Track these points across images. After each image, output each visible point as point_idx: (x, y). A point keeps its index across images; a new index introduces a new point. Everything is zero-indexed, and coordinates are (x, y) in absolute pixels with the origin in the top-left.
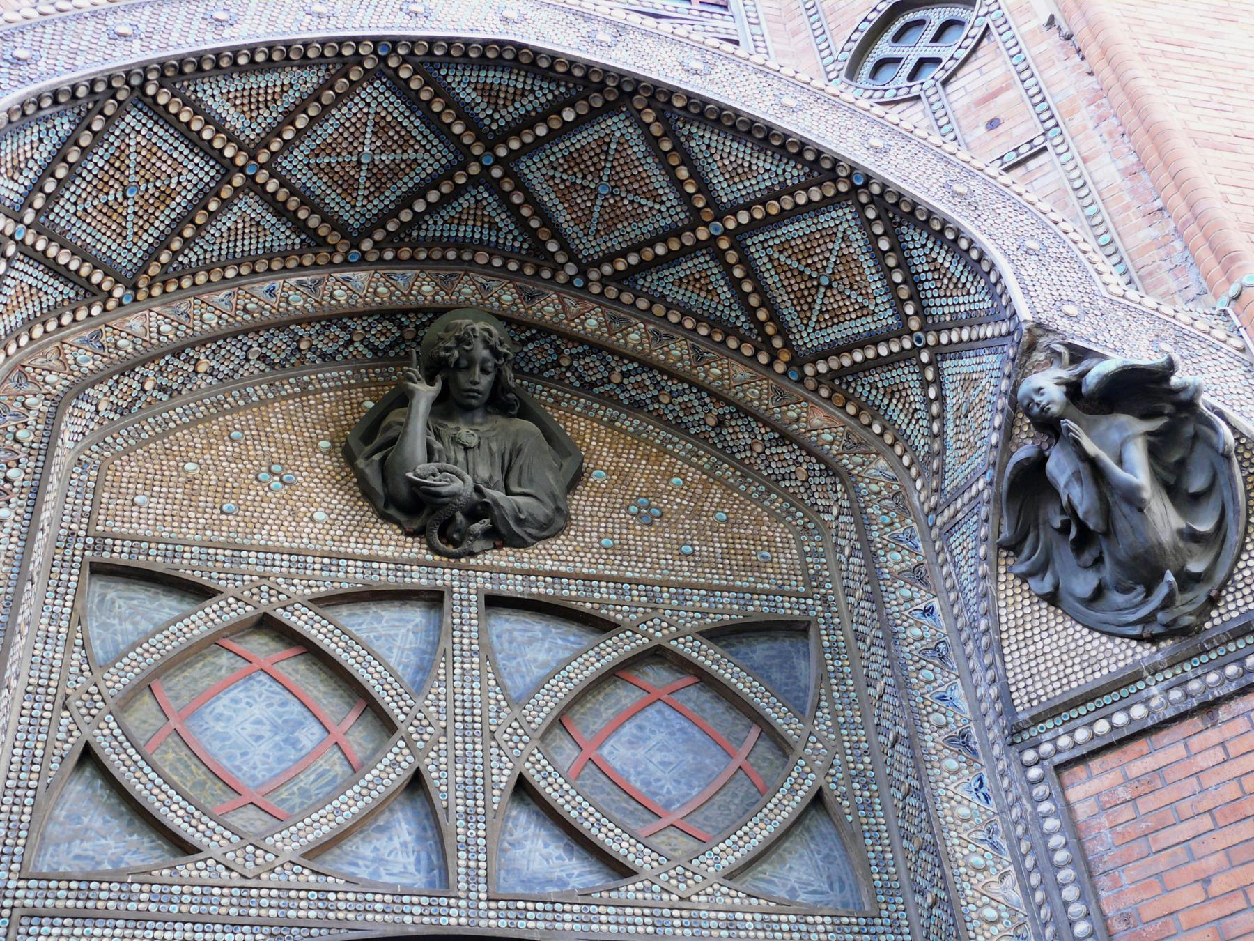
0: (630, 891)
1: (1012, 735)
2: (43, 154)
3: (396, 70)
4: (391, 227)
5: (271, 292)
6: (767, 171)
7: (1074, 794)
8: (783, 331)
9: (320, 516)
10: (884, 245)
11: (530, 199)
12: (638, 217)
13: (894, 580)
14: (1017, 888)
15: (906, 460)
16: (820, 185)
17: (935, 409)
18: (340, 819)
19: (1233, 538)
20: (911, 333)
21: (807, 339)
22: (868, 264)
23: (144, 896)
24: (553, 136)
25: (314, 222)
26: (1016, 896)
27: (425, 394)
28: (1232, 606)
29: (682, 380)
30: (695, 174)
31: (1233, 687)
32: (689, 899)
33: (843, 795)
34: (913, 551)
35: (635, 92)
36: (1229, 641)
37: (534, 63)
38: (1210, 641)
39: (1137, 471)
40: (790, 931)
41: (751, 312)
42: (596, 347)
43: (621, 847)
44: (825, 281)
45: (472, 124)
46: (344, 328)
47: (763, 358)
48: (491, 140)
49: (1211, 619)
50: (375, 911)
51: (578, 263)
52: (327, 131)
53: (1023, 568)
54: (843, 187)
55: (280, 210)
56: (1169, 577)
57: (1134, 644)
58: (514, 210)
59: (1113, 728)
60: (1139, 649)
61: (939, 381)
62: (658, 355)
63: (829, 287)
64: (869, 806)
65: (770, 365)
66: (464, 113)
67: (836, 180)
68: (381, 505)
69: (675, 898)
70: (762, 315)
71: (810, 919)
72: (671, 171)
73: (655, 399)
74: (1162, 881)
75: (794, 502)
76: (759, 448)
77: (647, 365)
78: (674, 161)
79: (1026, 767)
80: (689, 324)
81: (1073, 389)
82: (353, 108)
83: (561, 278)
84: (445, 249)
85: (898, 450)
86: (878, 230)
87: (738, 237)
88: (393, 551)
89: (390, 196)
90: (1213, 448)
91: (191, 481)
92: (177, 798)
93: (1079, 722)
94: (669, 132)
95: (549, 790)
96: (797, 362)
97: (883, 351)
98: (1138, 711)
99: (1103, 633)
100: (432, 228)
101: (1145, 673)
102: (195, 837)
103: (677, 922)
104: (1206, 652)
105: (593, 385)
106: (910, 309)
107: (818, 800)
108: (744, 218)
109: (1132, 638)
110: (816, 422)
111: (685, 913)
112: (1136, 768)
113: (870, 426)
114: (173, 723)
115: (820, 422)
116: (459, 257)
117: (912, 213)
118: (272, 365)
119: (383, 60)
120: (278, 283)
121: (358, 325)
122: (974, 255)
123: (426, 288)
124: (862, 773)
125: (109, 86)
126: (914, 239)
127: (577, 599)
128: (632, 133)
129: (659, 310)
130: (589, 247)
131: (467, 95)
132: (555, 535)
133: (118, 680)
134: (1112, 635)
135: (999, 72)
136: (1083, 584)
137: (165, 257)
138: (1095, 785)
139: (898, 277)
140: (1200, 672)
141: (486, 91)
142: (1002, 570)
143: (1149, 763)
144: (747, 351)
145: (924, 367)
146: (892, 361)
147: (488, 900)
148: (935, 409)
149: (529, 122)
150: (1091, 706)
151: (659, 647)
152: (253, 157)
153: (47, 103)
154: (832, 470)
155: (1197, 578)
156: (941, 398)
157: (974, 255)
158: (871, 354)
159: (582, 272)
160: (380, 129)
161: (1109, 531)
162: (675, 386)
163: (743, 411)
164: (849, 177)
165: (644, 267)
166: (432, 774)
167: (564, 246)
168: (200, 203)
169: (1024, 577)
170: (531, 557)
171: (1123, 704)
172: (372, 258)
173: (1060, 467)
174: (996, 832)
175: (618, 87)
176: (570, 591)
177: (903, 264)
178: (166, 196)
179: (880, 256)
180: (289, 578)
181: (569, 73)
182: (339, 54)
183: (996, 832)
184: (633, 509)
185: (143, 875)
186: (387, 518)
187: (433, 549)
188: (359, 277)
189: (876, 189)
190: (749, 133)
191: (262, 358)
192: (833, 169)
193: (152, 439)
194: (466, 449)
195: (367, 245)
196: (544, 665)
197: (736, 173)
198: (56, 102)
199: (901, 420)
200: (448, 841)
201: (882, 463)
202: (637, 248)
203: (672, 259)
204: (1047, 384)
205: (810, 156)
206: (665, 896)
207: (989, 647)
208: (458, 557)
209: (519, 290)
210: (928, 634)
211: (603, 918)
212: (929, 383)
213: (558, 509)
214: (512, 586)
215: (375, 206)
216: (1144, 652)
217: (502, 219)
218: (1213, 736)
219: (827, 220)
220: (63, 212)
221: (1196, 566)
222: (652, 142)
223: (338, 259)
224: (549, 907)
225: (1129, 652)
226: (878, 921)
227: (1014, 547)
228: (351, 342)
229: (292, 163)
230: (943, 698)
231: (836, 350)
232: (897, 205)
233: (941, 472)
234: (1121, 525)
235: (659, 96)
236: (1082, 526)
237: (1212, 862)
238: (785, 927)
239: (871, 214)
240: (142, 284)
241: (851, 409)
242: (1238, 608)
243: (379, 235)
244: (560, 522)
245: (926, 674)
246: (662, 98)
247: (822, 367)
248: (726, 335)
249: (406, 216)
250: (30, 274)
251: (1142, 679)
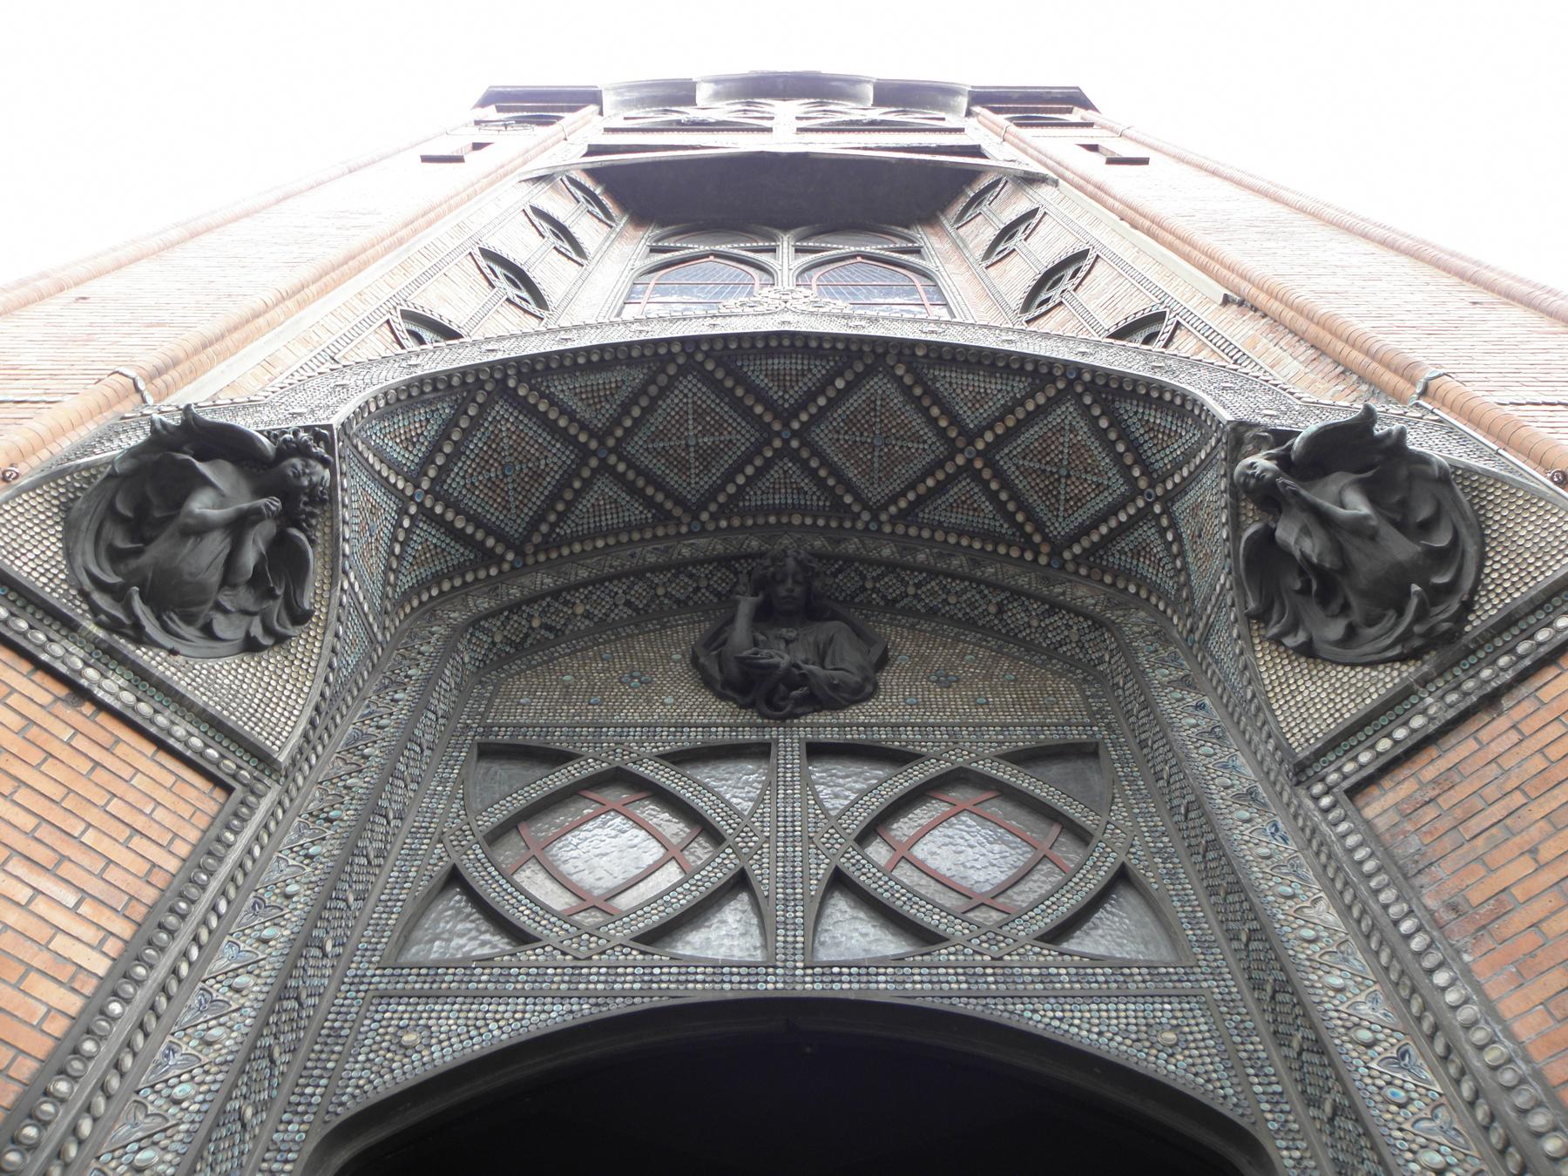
0: (943, 954)
1: (1296, 774)
2: (432, 430)
3: (702, 364)
4: (722, 499)
5: (633, 556)
6: (998, 391)
8: (1040, 527)
9: (669, 700)
10: (1104, 423)
11: (825, 462)
12: (908, 460)
13: (1164, 687)
14: (1332, 910)
15: (1161, 606)
16: (1042, 390)
17: (1175, 549)
18: (669, 910)
19: (1471, 550)
20: (1142, 492)
21: (1060, 527)
22: (1094, 445)
23: (484, 978)
24: (833, 403)
25: (660, 497)
26: (1332, 918)
27: (746, 606)
28: (1488, 607)
29: (963, 579)
30: (946, 411)
31: (1508, 676)
32: (1001, 959)
33: (1146, 868)
34: (1179, 667)
35: (886, 353)
36: (1493, 637)
37: (806, 346)
38: (1475, 640)
39: (1358, 506)
40: (1106, 982)
41: (1010, 517)
42: (891, 566)
43: (933, 920)
44: (1063, 472)
45: (770, 405)
46: (691, 576)
47: (1029, 556)
48: (787, 416)
49: (1470, 622)
50: (696, 982)
51: (870, 509)
52: (657, 420)
53: (1274, 631)
54: (1061, 385)
55: (632, 489)
56: (1415, 588)
57: (1397, 665)
58: (813, 473)
59: (1396, 742)
60: (1404, 668)
61: (1173, 525)
62: (942, 565)
63: (1068, 476)
64: (1172, 875)
65: (1035, 560)
66: (761, 396)
67: (1054, 380)
68: (718, 687)
69: (987, 958)
70: (1020, 518)
71: (1126, 971)
72: (925, 411)
73: (945, 601)
74: (1484, 863)
75: (1072, 663)
76: (1035, 623)
77: (933, 573)
78: (926, 402)
79: (1316, 799)
80: (964, 542)
81: (1284, 461)
82: (675, 398)
83: (860, 525)
84: (767, 516)
85: (1153, 600)
86: (1096, 412)
87: (987, 455)
89: (716, 473)
90: (1428, 478)
91: (567, 687)
92: (525, 901)
93: (1360, 748)
94: (919, 380)
95: (863, 878)
96: (1056, 552)
97: (1123, 517)
98: (1417, 722)
99: (1365, 665)
100: (754, 499)
101: (1416, 687)
103: (991, 979)
104: (1474, 652)
105: (895, 601)
106: (1136, 472)
107: (1122, 877)
108: (989, 437)
109: (1393, 660)
110: (1080, 593)
111: (999, 971)
112: (1430, 773)
113: (1126, 589)
114: (532, 852)
115: (1085, 595)
116: (779, 521)
117: (1121, 387)
118: (636, 610)
119: (690, 356)
120: (638, 550)
121: (702, 571)
122: (1178, 401)
123: (754, 543)
124: (1160, 851)
125: (478, 379)
126: (1127, 409)
127: (886, 740)
128: (891, 388)
129: (939, 536)
130: (876, 494)
131: (762, 381)
132: (867, 699)
133: (487, 821)
134: (1373, 665)
136: (1336, 630)
137: (544, 528)
138: (1391, 798)
139: (1121, 448)
140: (1472, 672)
141: (775, 376)
142: (1257, 641)
143: (1443, 764)
144: (1015, 553)
145: (1158, 517)
146: (1133, 522)
147: (804, 968)
148: (1175, 549)
149: (811, 397)
150: (1369, 730)
151: (961, 769)
152: (602, 443)
153: (428, 389)
154: (1098, 624)
155: (1450, 589)
156: (1178, 538)
157: (1178, 401)
158: (1113, 523)
159: (875, 518)
160: (699, 416)
161: (1346, 568)
162: (957, 586)
163: (1017, 593)
164: (1064, 375)
165: (921, 501)
166: (755, 870)
167: (858, 498)
168: (564, 483)
169: (1277, 640)
170: (842, 716)
171: (1401, 720)
172: (711, 527)
173: (1287, 532)
174: (1301, 866)
175: (873, 351)
176: (882, 735)
177: (1124, 435)
178: (537, 475)
179: (1101, 434)
180: (640, 744)
181: (834, 348)
182: (656, 354)
183: (1301, 866)
184: (933, 678)
185: (486, 961)
186: (722, 697)
187: (762, 715)
188: (701, 542)
189: (1087, 377)
190: (979, 363)
191: (628, 604)
192: (1050, 373)
193: (539, 664)
194: (788, 642)
195: (705, 516)
196: (859, 791)
197: (976, 400)
198: (435, 389)
199: (1150, 572)
200: (767, 921)
201: (1142, 614)
202: (912, 486)
203: (941, 488)
204: (1261, 462)
205: (1029, 367)
206: (978, 958)
207: (1259, 709)
208: (783, 719)
209: (829, 539)
210: (1203, 723)
211: (917, 978)
212: (1166, 529)
213: (866, 679)
214: (829, 735)
215: (706, 482)
216: (1409, 671)
217: (806, 484)
218: (1502, 723)
219: (1054, 419)
220: (455, 483)
221: (1442, 579)
222: (906, 390)
223: (684, 529)
224: (863, 971)
225: (1395, 673)
226: (1197, 970)
227: (1262, 617)
228: (698, 589)
229: (636, 446)
230: (1225, 767)
231: (1085, 530)
232: (1107, 385)
233: (1190, 598)
234: (1356, 556)
235: (903, 349)
236: (1318, 570)
237: (1534, 833)
238: (1102, 979)
239: (1088, 400)
240: (529, 549)
241: (1108, 579)
242: (1494, 606)
243: (713, 507)
244: (869, 688)
245: (1207, 749)
246: (907, 352)
247: (1077, 549)
248: (996, 545)
249: (731, 489)
250: (434, 537)
251: (1415, 693)
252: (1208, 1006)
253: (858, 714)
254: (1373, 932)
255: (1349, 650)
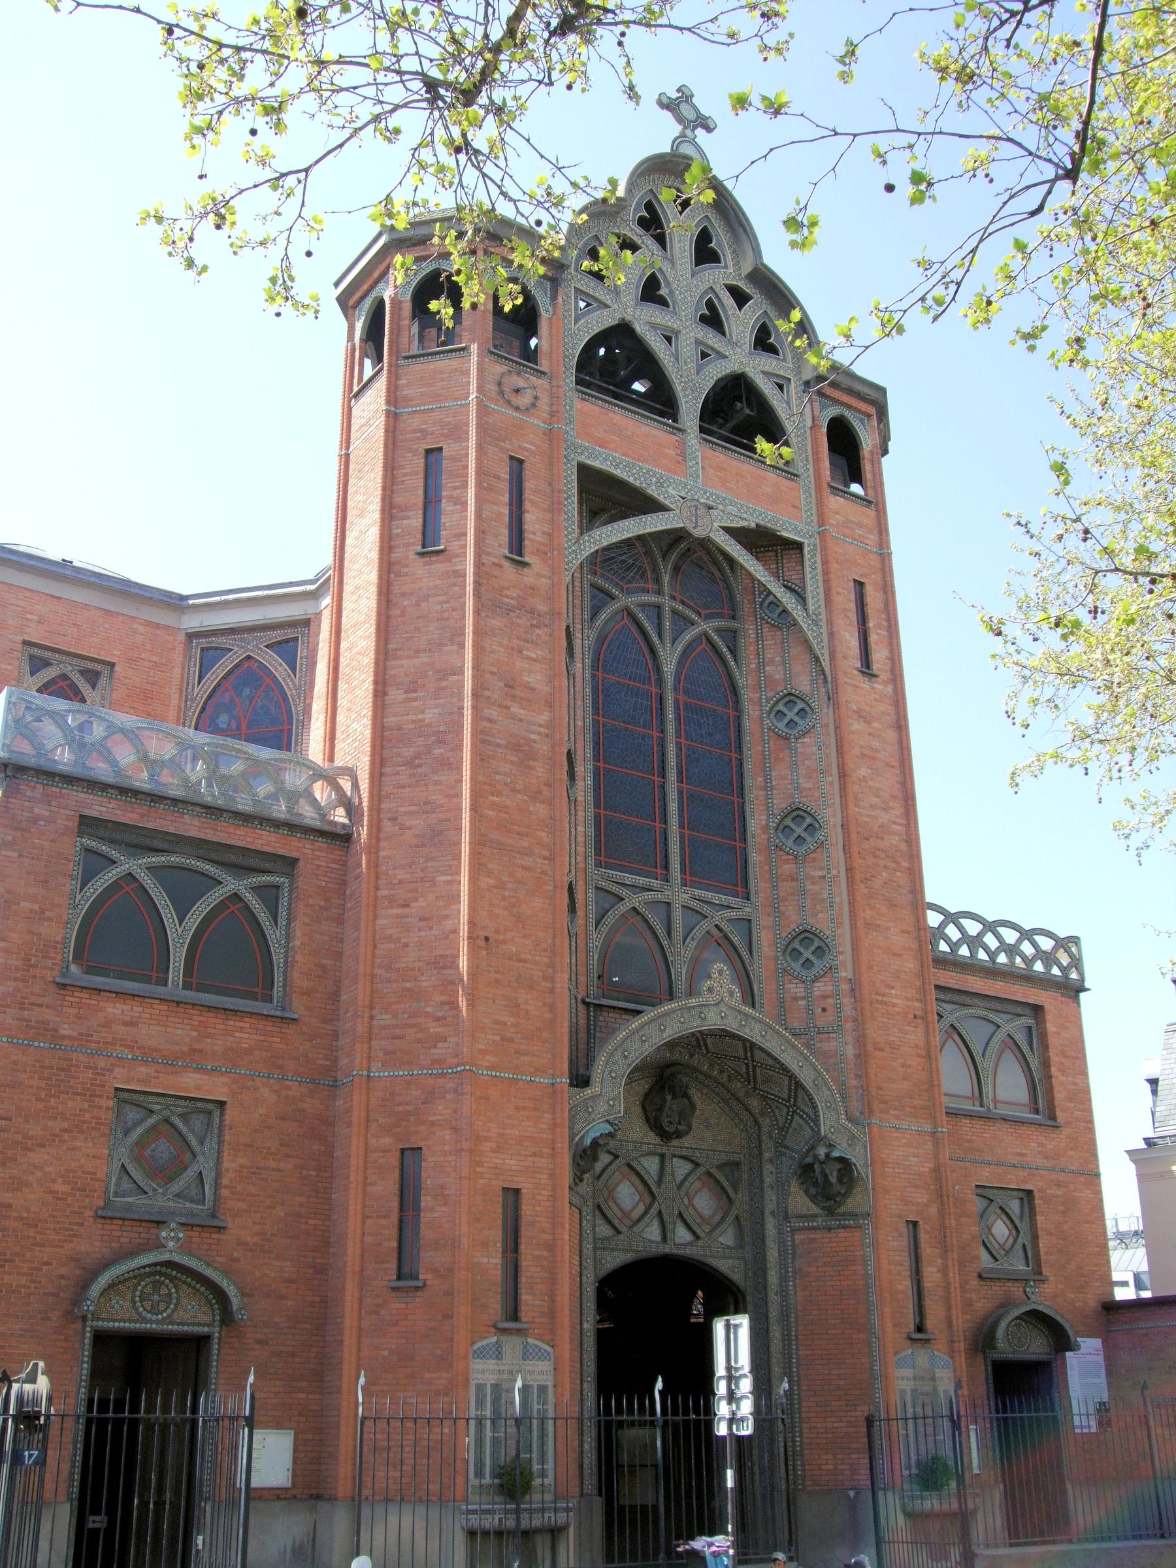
0: (700, 1243)
7: (796, 1237)
8: (755, 1083)
81: (827, 1155)
88: (653, 1138)
102: (621, 1229)
126: (801, 1093)
135: (830, 988)
218: (828, 1235)
252: (745, 1262)
253: (686, 1141)
254: (783, 1265)
255: (813, 1198)
